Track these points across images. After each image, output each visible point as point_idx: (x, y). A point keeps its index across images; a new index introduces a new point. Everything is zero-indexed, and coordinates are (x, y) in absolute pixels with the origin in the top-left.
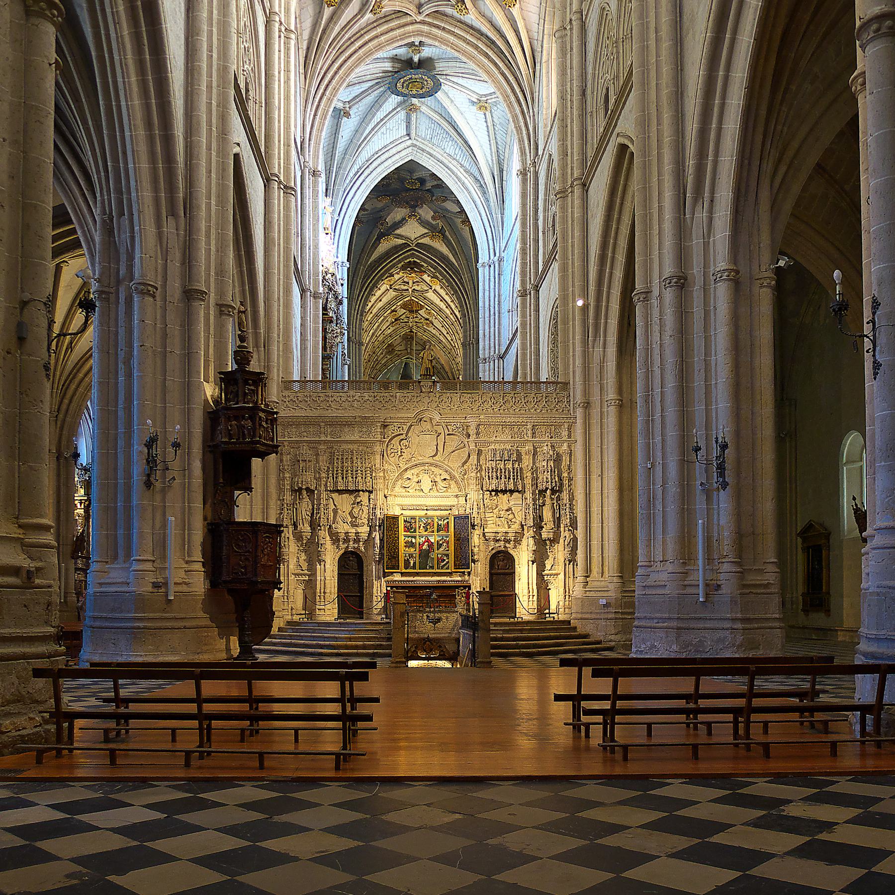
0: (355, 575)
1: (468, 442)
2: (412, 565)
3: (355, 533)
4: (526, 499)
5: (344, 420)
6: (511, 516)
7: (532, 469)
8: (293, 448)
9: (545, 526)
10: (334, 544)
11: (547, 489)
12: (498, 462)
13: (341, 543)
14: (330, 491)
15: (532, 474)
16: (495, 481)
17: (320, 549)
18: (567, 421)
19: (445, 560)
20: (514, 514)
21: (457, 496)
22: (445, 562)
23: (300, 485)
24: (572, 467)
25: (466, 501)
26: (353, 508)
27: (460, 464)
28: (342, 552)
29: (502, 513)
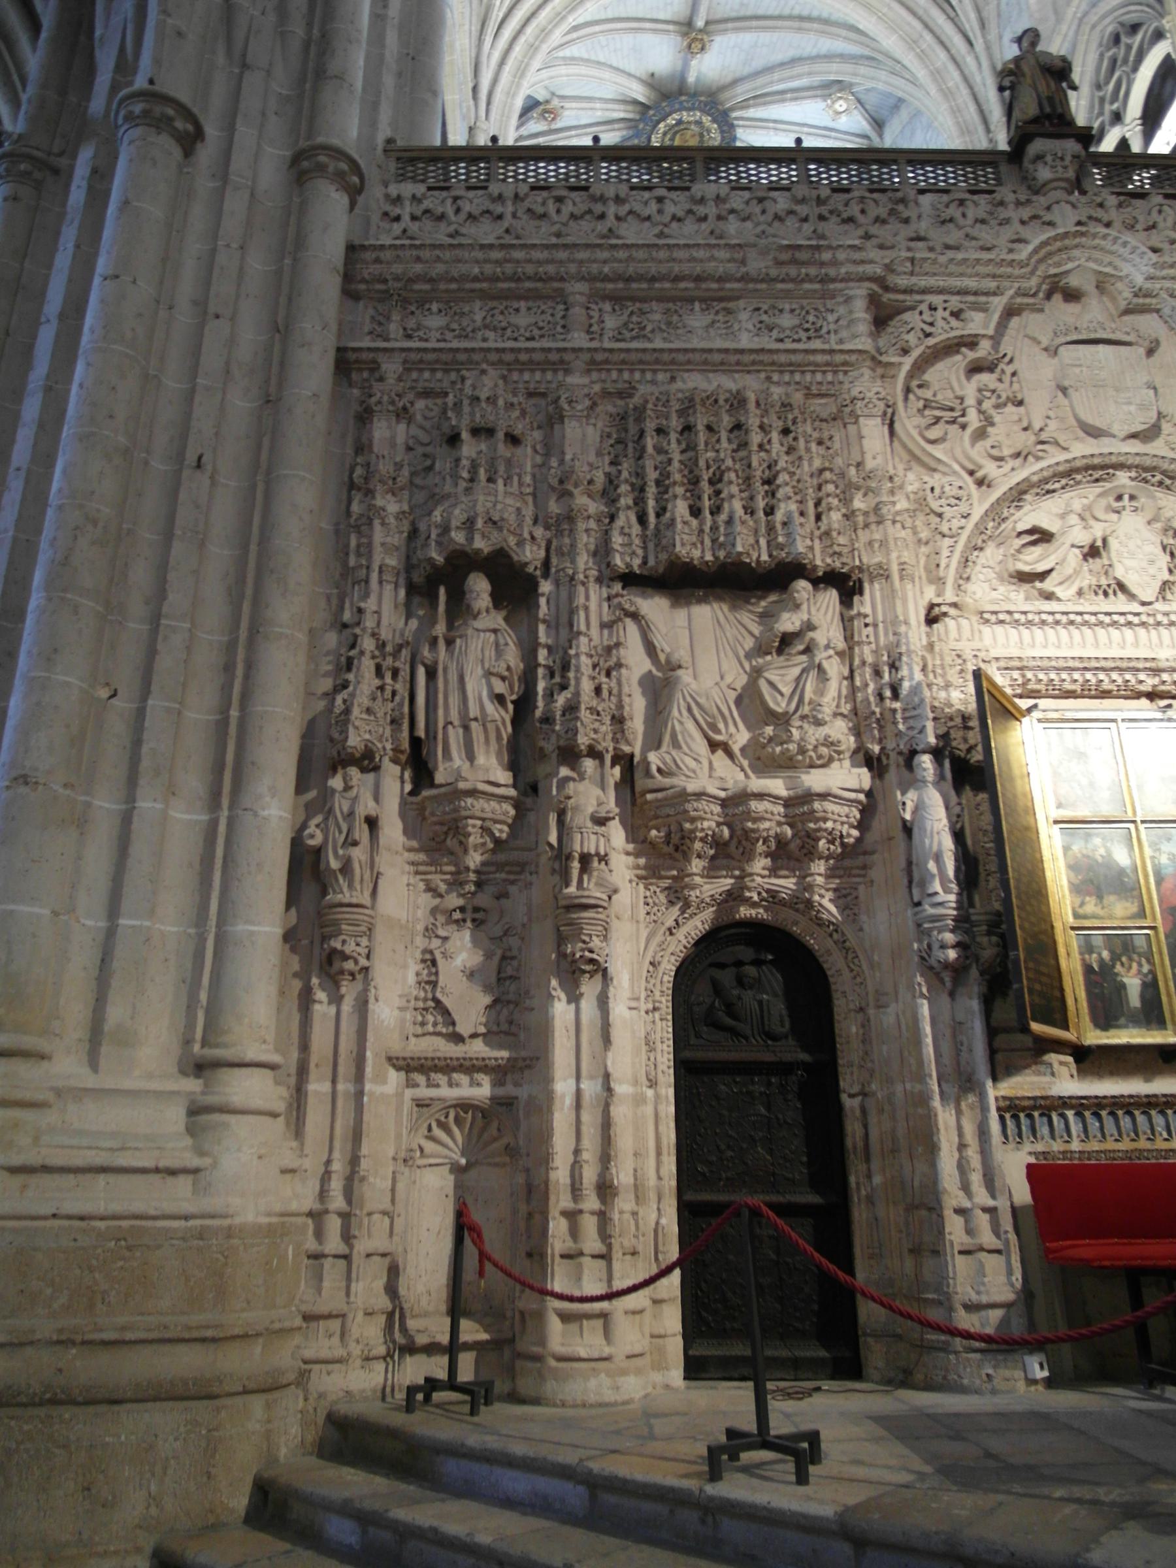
0: (785, 1069)
2: (1134, 998)
3: (788, 803)
5: (686, 268)
8: (427, 394)
10: (650, 874)
13: (696, 865)
14: (630, 580)
17: (572, 889)
23: (459, 537)
26: (757, 673)
28: (697, 925)
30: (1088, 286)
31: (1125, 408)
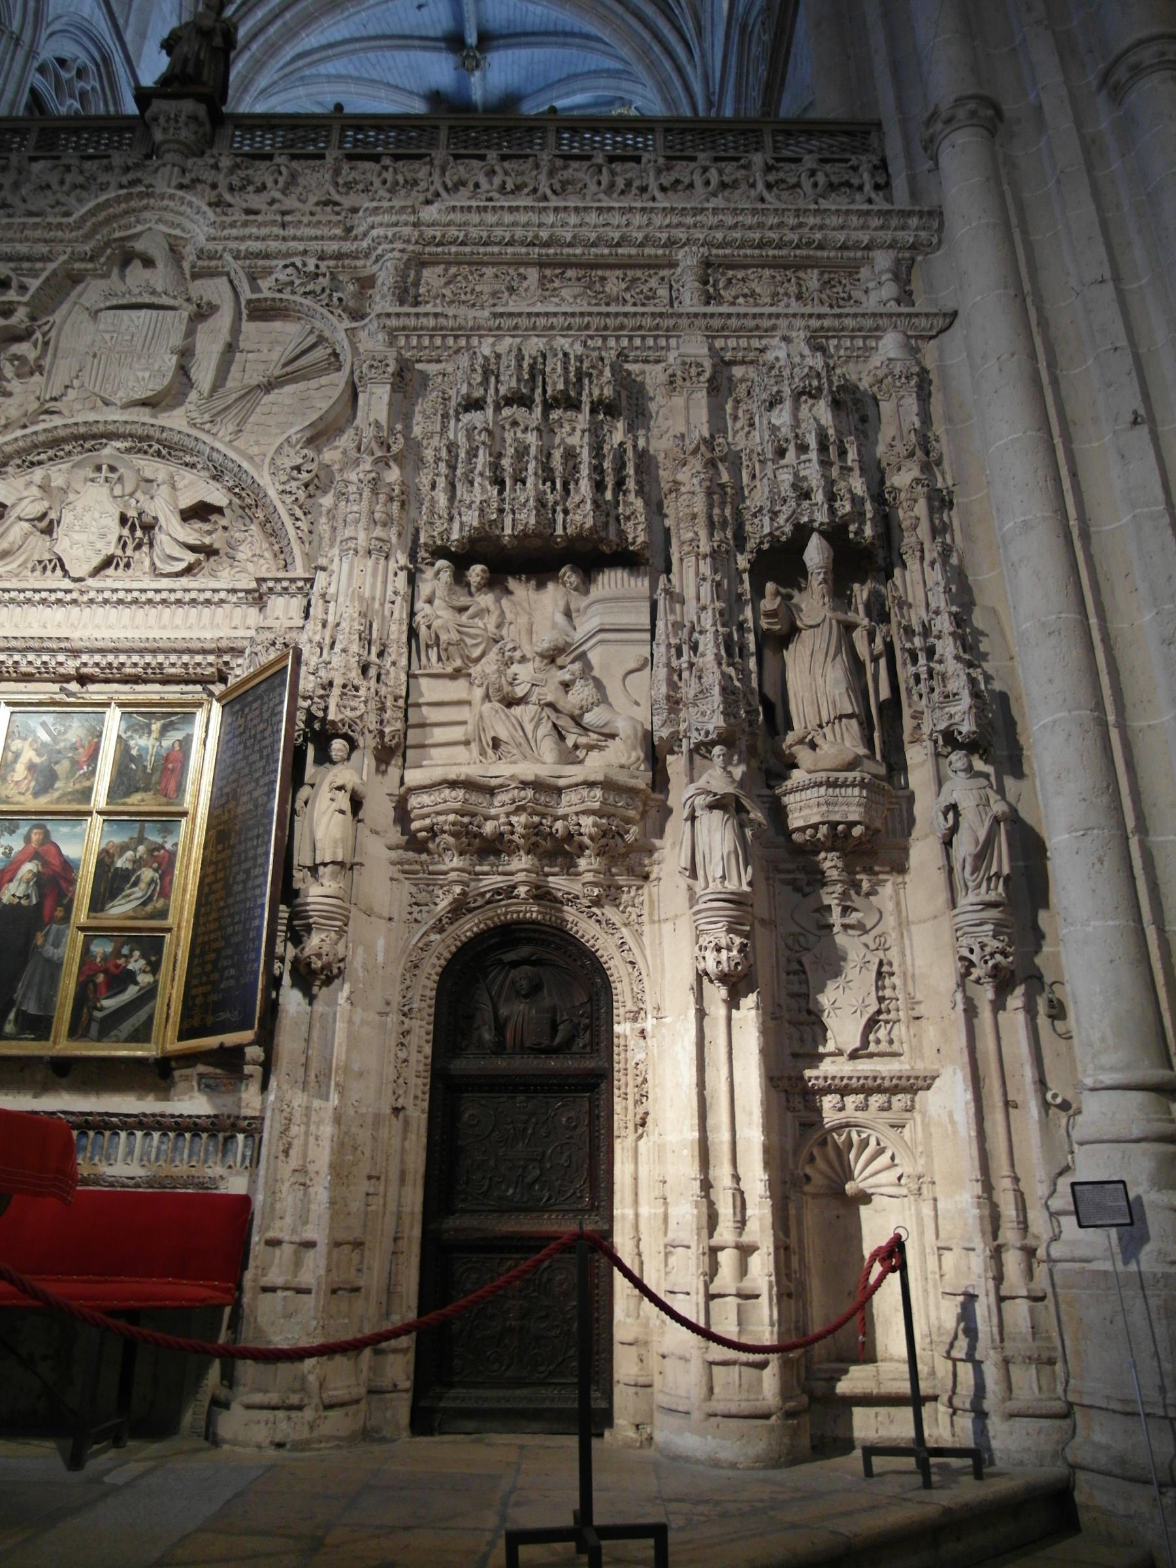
1: (351, 333)
4: (676, 598)
6: (581, 694)
7: (709, 443)
9: (803, 755)
11: (802, 533)
12: (506, 412)
15: (711, 464)
16: (481, 491)
18: (886, 236)
19: (130, 977)
20: (599, 685)
21: (258, 598)
22: (132, 992)
24: (944, 447)
25: (307, 616)
27: (296, 429)
29: (524, 673)
30: (158, 252)
31: (140, 374)
